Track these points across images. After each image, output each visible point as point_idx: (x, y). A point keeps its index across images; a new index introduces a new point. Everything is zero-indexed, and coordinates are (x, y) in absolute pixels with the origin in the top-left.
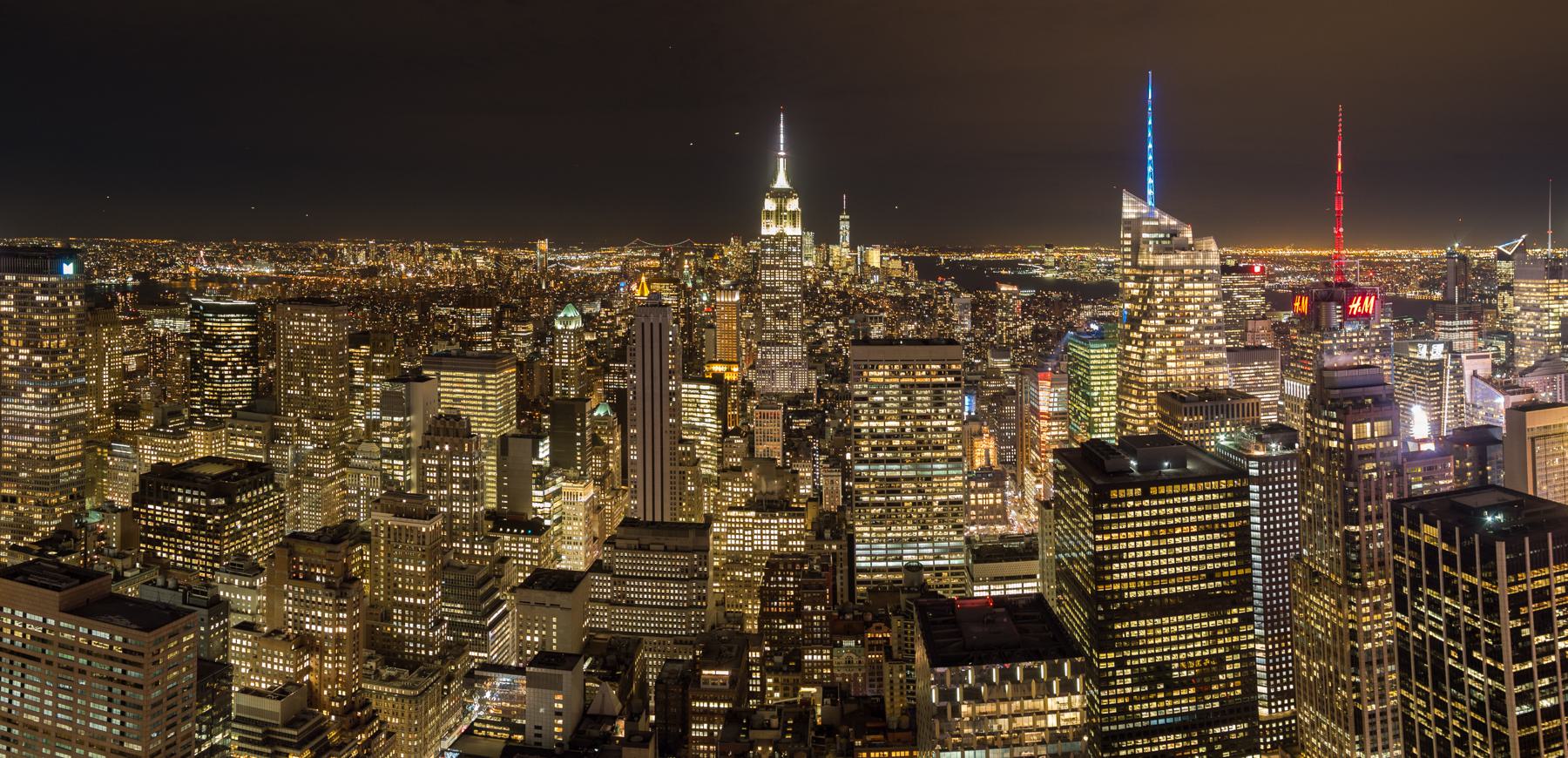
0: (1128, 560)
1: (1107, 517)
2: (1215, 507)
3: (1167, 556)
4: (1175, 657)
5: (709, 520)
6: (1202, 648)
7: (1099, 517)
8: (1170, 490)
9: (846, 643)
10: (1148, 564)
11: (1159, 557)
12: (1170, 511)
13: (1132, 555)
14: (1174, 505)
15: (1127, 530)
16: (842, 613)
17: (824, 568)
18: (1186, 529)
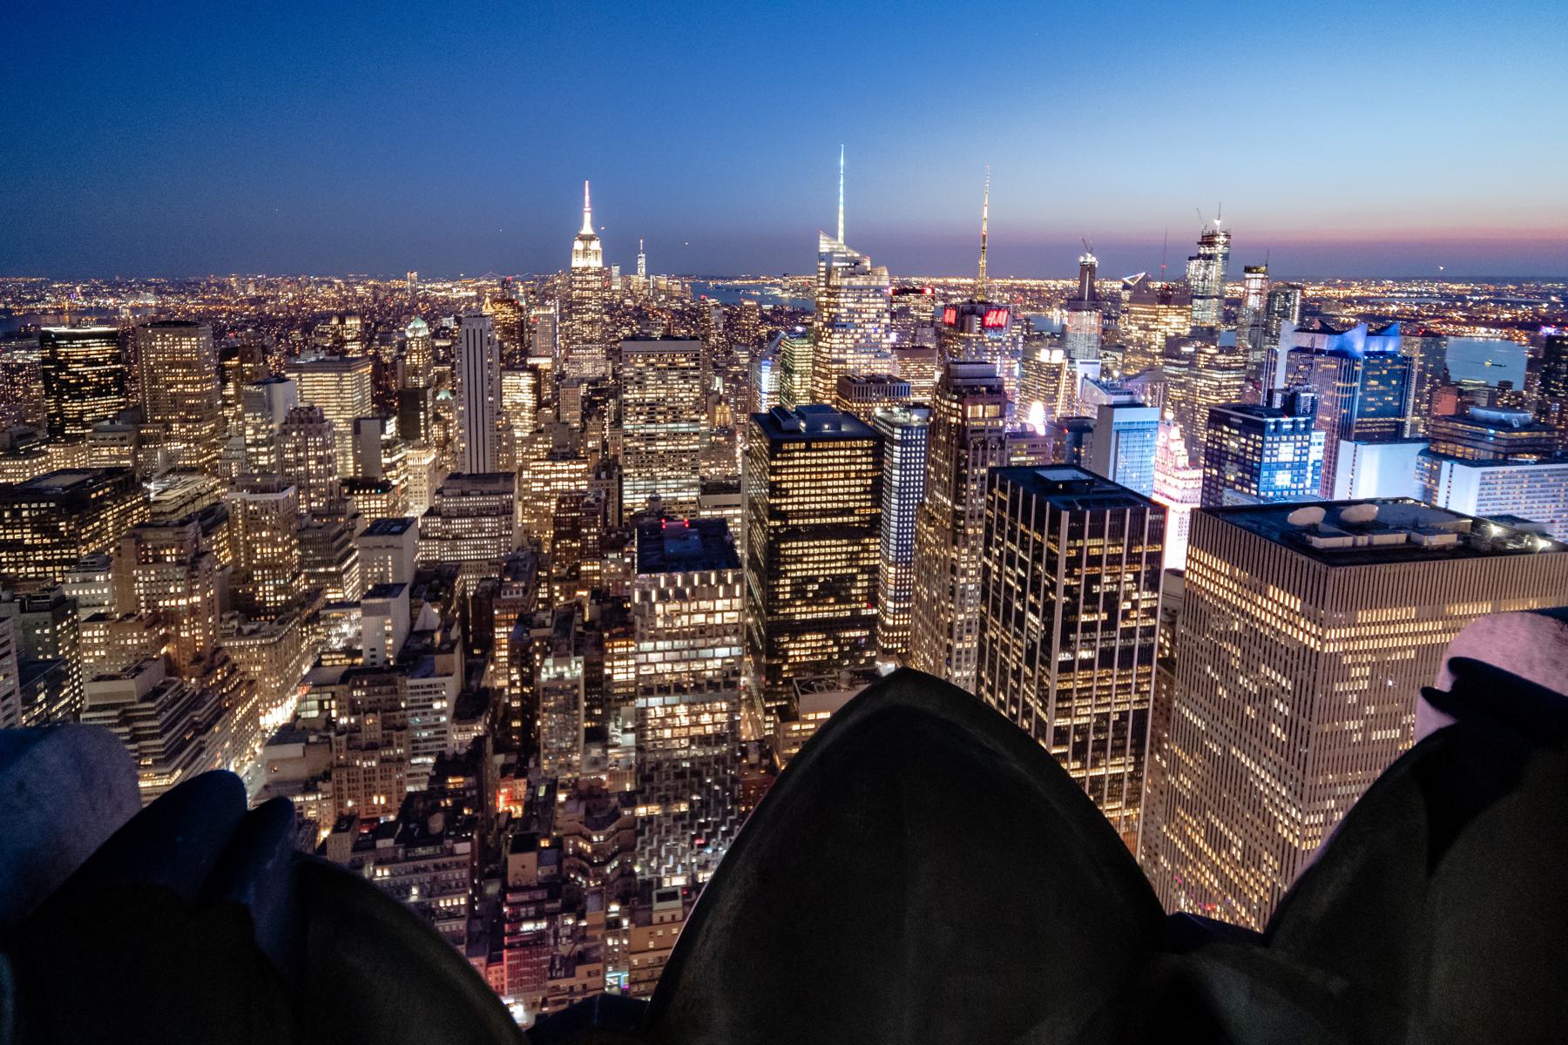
0: (793, 496)
1: (779, 463)
2: (859, 460)
3: (821, 495)
4: (822, 572)
5: (521, 469)
6: (841, 568)
7: (774, 463)
8: (826, 445)
9: (610, 556)
10: (807, 499)
11: (815, 495)
12: (825, 461)
13: (796, 492)
14: (828, 457)
15: (793, 474)
16: (609, 533)
17: (598, 500)
18: (836, 475)
